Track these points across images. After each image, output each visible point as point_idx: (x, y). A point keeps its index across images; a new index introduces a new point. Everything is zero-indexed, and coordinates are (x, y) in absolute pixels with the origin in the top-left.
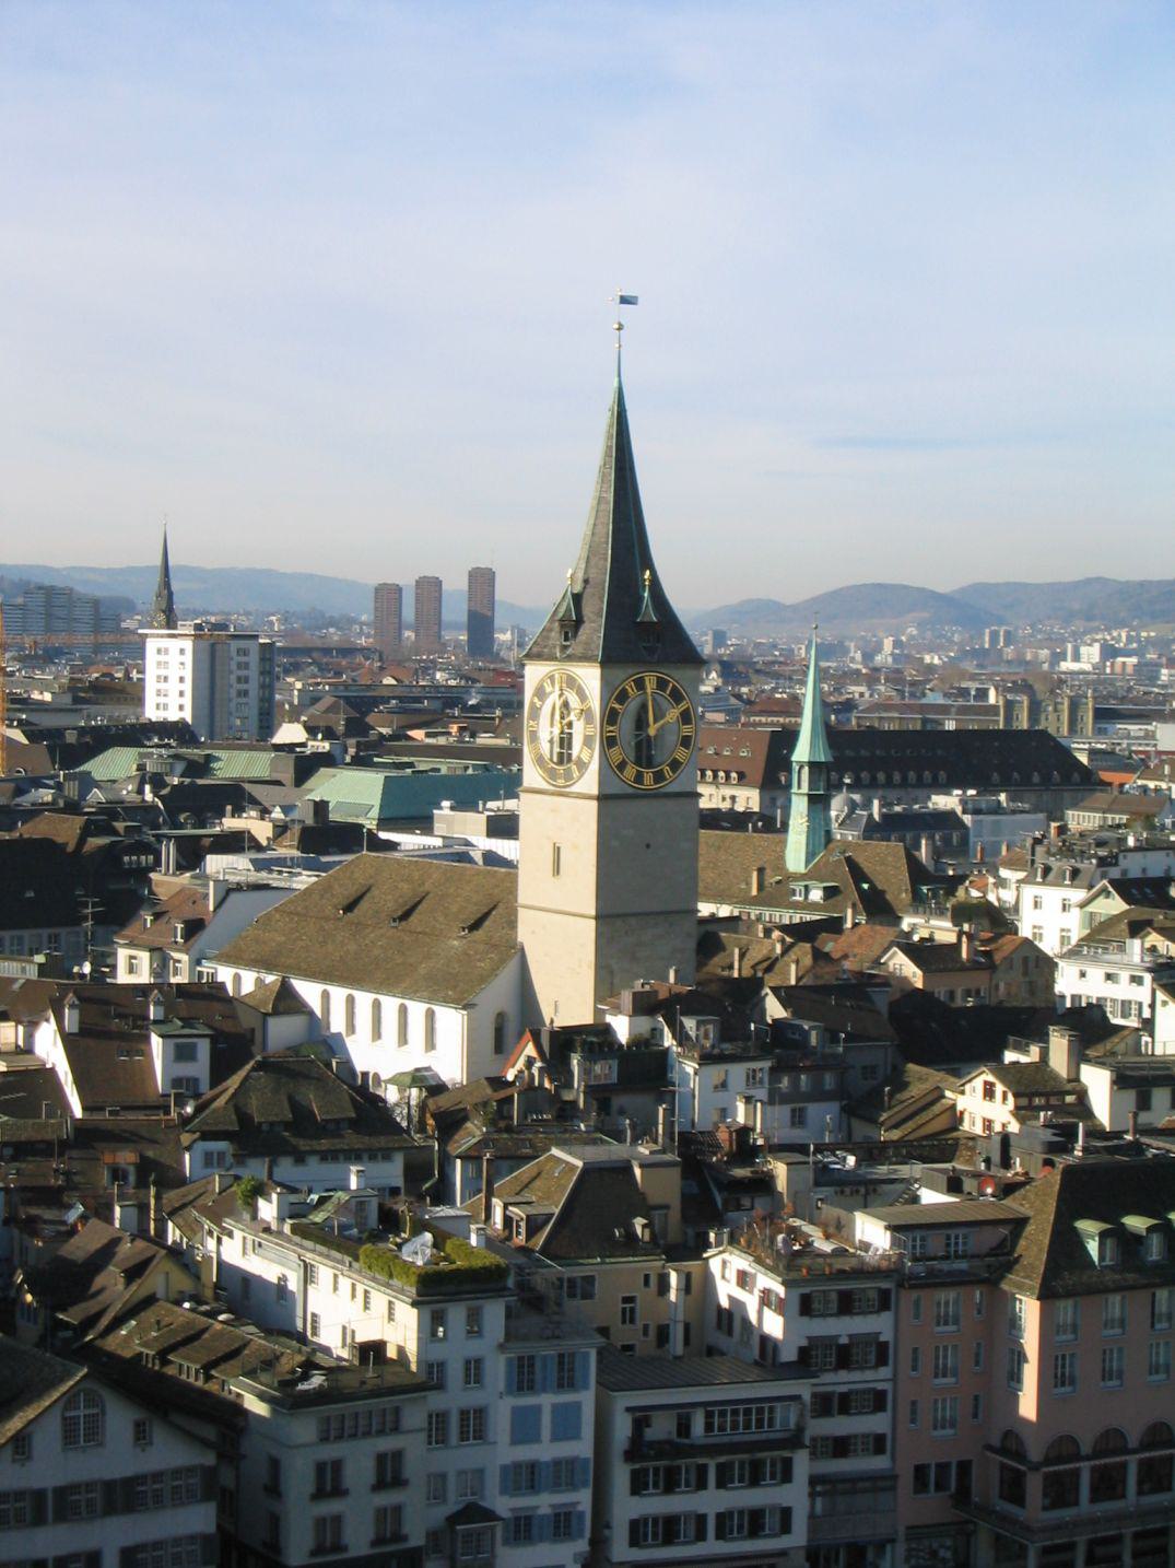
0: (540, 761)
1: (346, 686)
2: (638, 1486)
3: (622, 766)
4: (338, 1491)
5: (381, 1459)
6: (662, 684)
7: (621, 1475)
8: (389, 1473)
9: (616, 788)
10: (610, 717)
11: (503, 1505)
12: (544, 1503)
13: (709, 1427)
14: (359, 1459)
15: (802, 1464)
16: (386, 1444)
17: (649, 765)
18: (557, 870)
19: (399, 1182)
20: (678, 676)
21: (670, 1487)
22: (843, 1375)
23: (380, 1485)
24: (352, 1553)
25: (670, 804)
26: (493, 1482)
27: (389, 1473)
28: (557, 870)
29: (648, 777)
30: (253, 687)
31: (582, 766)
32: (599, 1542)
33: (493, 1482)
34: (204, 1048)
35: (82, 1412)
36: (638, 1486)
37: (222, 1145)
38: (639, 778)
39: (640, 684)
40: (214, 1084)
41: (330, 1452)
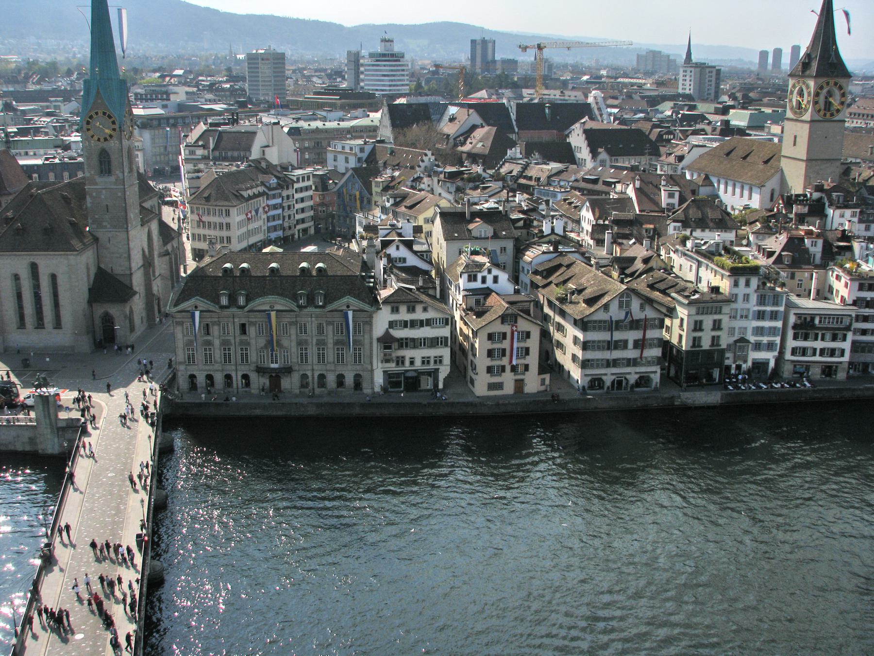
0: (792, 108)
1: (745, 84)
2: (795, 337)
3: (819, 111)
4: (701, 330)
5: (715, 321)
6: (836, 84)
7: (790, 333)
8: (717, 325)
9: (817, 118)
10: (817, 94)
11: (752, 339)
12: (765, 339)
13: (820, 322)
14: (708, 321)
15: (850, 336)
16: (717, 317)
17: (829, 110)
18: (795, 144)
19: (734, 239)
20: (842, 81)
21: (806, 338)
22: (867, 310)
23: (714, 329)
24: (704, 348)
25: (835, 124)
26: (749, 331)
27: (717, 325)
28: (795, 144)
29: (828, 114)
30: (713, 83)
31: (806, 110)
32: (782, 352)
33: (749, 331)
34: (677, 195)
35: (625, 299)
36: (795, 337)
37: (679, 224)
38: (825, 115)
39: (828, 84)
40: (680, 204)
41: (699, 318)
